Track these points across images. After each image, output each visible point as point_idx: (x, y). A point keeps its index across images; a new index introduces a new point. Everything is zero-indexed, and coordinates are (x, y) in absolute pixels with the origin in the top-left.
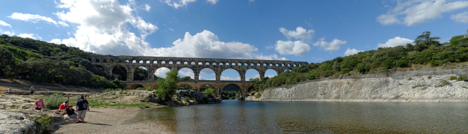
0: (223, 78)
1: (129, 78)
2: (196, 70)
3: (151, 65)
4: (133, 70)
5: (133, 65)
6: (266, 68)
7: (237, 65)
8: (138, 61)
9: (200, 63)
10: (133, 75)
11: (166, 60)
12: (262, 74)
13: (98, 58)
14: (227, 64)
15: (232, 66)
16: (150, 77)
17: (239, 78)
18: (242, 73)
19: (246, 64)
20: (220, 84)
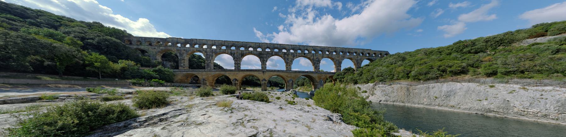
0: (294, 68)
1: (181, 66)
2: (263, 57)
3: (208, 50)
4: (187, 58)
5: (187, 50)
6: (343, 58)
7: (310, 52)
8: (192, 45)
9: (268, 50)
10: (187, 63)
11: (226, 44)
12: (338, 64)
13: (140, 40)
14: (299, 51)
15: (305, 54)
16: (208, 65)
17: (311, 69)
18: (316, 63)
19: (320, 52)
20: (293, 75)
